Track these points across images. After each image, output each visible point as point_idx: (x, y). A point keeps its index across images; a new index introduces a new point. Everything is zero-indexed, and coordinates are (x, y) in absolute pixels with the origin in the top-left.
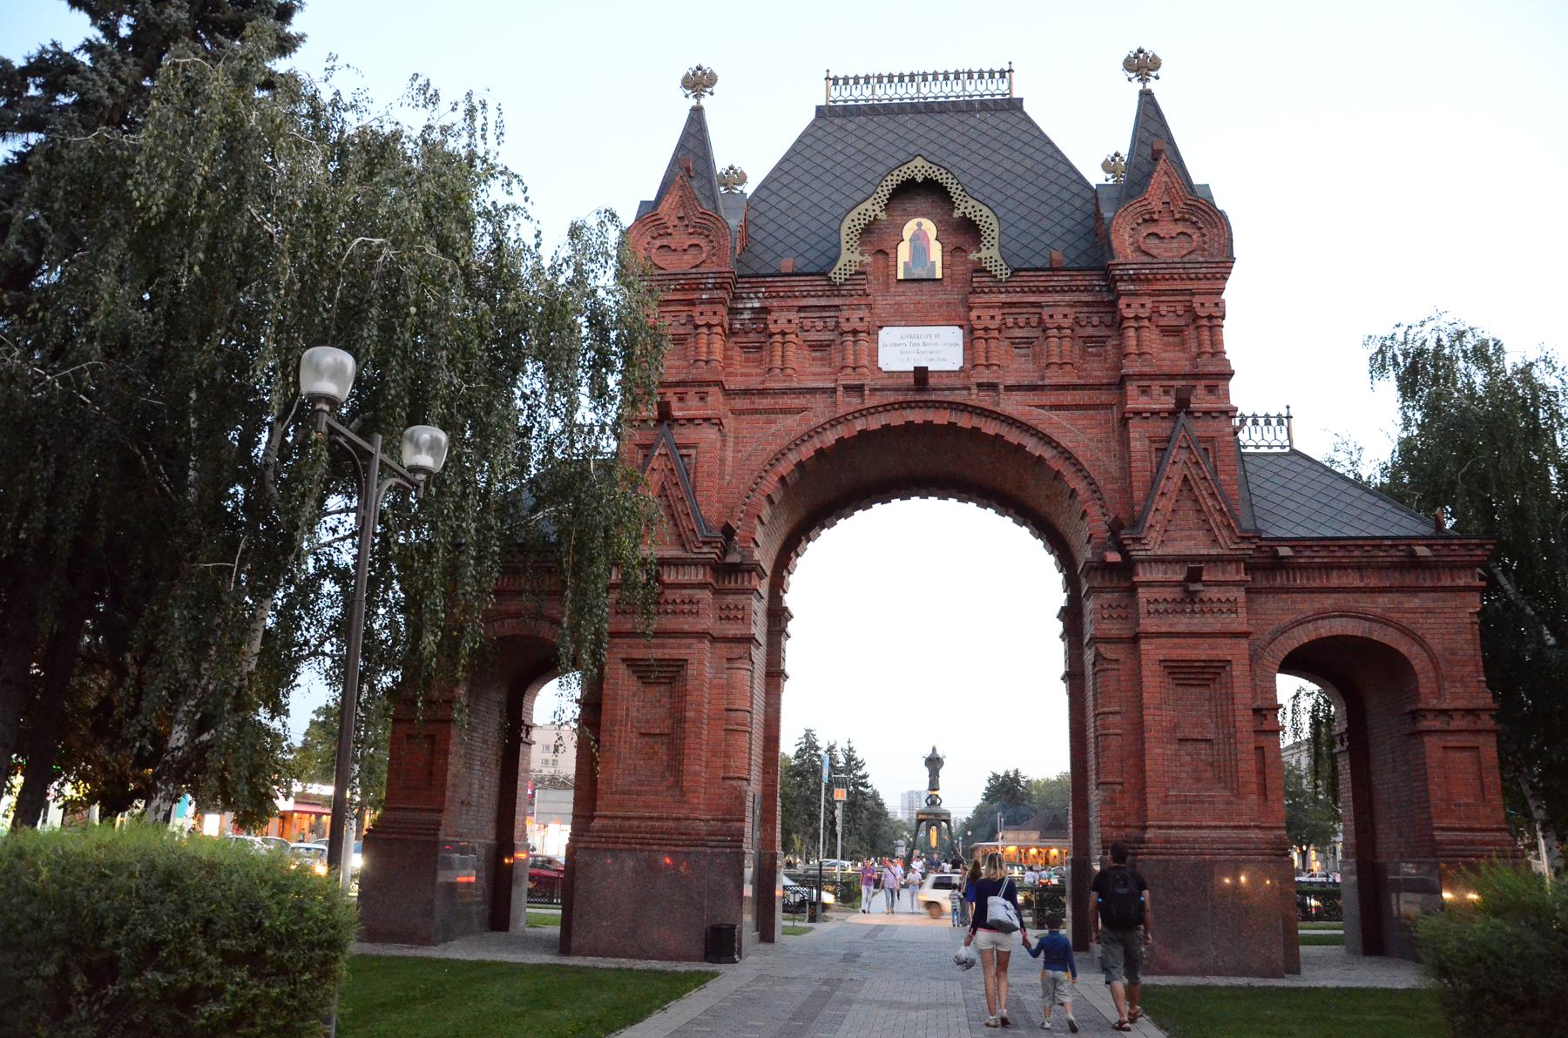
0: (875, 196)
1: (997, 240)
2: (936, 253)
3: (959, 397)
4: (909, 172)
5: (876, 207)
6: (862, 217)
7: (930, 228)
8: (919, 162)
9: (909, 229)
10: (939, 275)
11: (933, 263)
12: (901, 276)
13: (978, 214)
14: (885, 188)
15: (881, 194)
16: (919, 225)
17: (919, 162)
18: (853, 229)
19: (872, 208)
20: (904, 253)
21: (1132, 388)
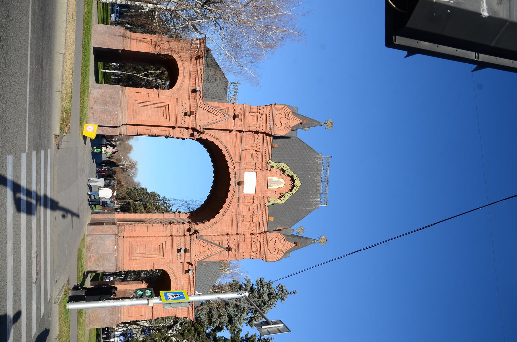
0: (291, 172)
1: (277, 203)
2: (275, 187)
3: (236, 193)
4: (297, 181)
5: (288, 172)
6: (286, 168)
7: (281, 186)
8: (300, 184)
9: (282, 180)
10: (268, 188)
11: (272, 186)
12: (269, 178)
13: (284, 199)
14: (293, 175)
15: (292, 174)
16: (283, 183)
17: (300, 184)
18: (283, 166)
19: (288, 171)
20: (275, 179)
21: (236, 236)
